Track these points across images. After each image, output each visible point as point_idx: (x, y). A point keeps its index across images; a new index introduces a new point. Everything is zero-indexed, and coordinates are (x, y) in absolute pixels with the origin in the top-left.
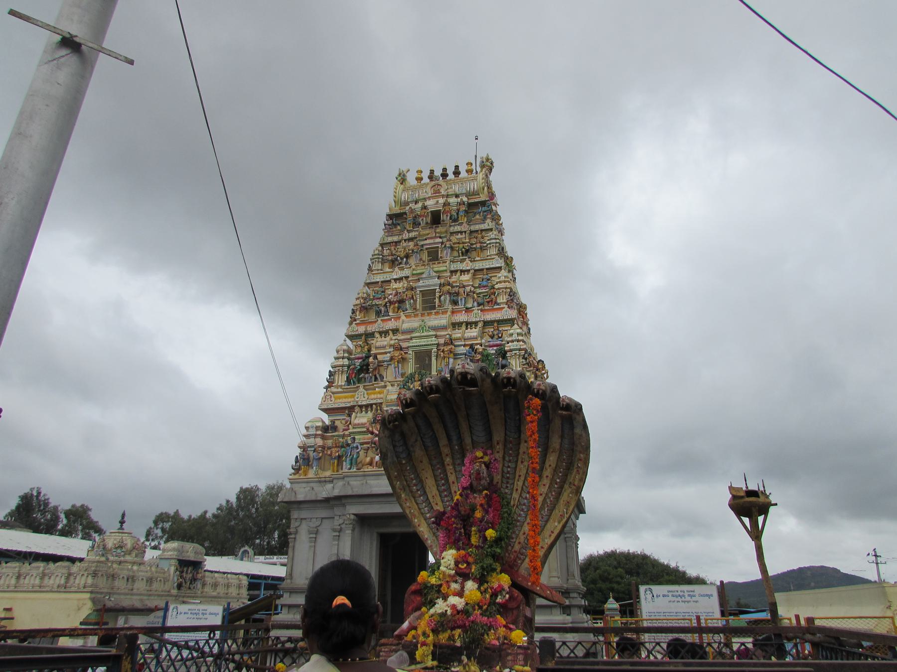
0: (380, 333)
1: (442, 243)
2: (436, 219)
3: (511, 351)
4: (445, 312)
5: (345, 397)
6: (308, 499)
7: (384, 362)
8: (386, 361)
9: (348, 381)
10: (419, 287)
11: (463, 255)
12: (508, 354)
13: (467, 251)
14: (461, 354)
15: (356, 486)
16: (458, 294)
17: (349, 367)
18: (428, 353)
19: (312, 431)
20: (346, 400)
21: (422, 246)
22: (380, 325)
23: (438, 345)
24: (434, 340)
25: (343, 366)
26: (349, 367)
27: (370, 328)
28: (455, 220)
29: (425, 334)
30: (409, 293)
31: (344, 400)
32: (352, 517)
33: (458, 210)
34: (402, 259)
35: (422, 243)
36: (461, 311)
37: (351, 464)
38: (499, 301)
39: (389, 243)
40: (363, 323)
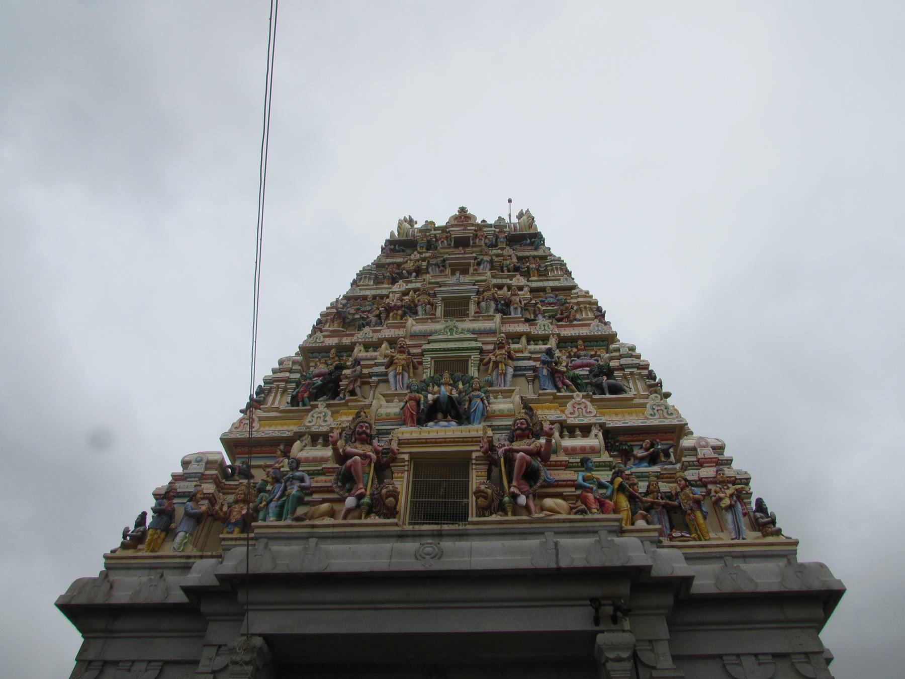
0: (367, 346)
1: (476, 258)
2: (462, 242)
3: (622, 368)
4: (491, 318)
5: (282, 425)
6: (140, 600)
7: (370, 375)
8: (377, 375)
9: (294, 401)
10: (441, 292)
11: (509, 271)
12: (616, 373)
13: (516, 269)
14: (526, 368)
15: (286, 557)
16: (508, 304)
17: (298, 383)
18: (463, 363)
19: (194, 468)
20: (285, 428)
21: (444, 260)
22: (368, 333)
23: (482, 351)
24: (473, 344)
25: (287, 381)
26: (298, 383)
27: (346, 341)
28: (494, 246)
29: (456, 336)
30: (424, 298)
31: (280, 428)
32: (258, 642)
33: (497, 238)
34: (410, 273)
35: (446, 256)
36: (518, 322)
37: (279, 517)
38: (578, 316)
39: (389, 264)
40: (334, 334)
